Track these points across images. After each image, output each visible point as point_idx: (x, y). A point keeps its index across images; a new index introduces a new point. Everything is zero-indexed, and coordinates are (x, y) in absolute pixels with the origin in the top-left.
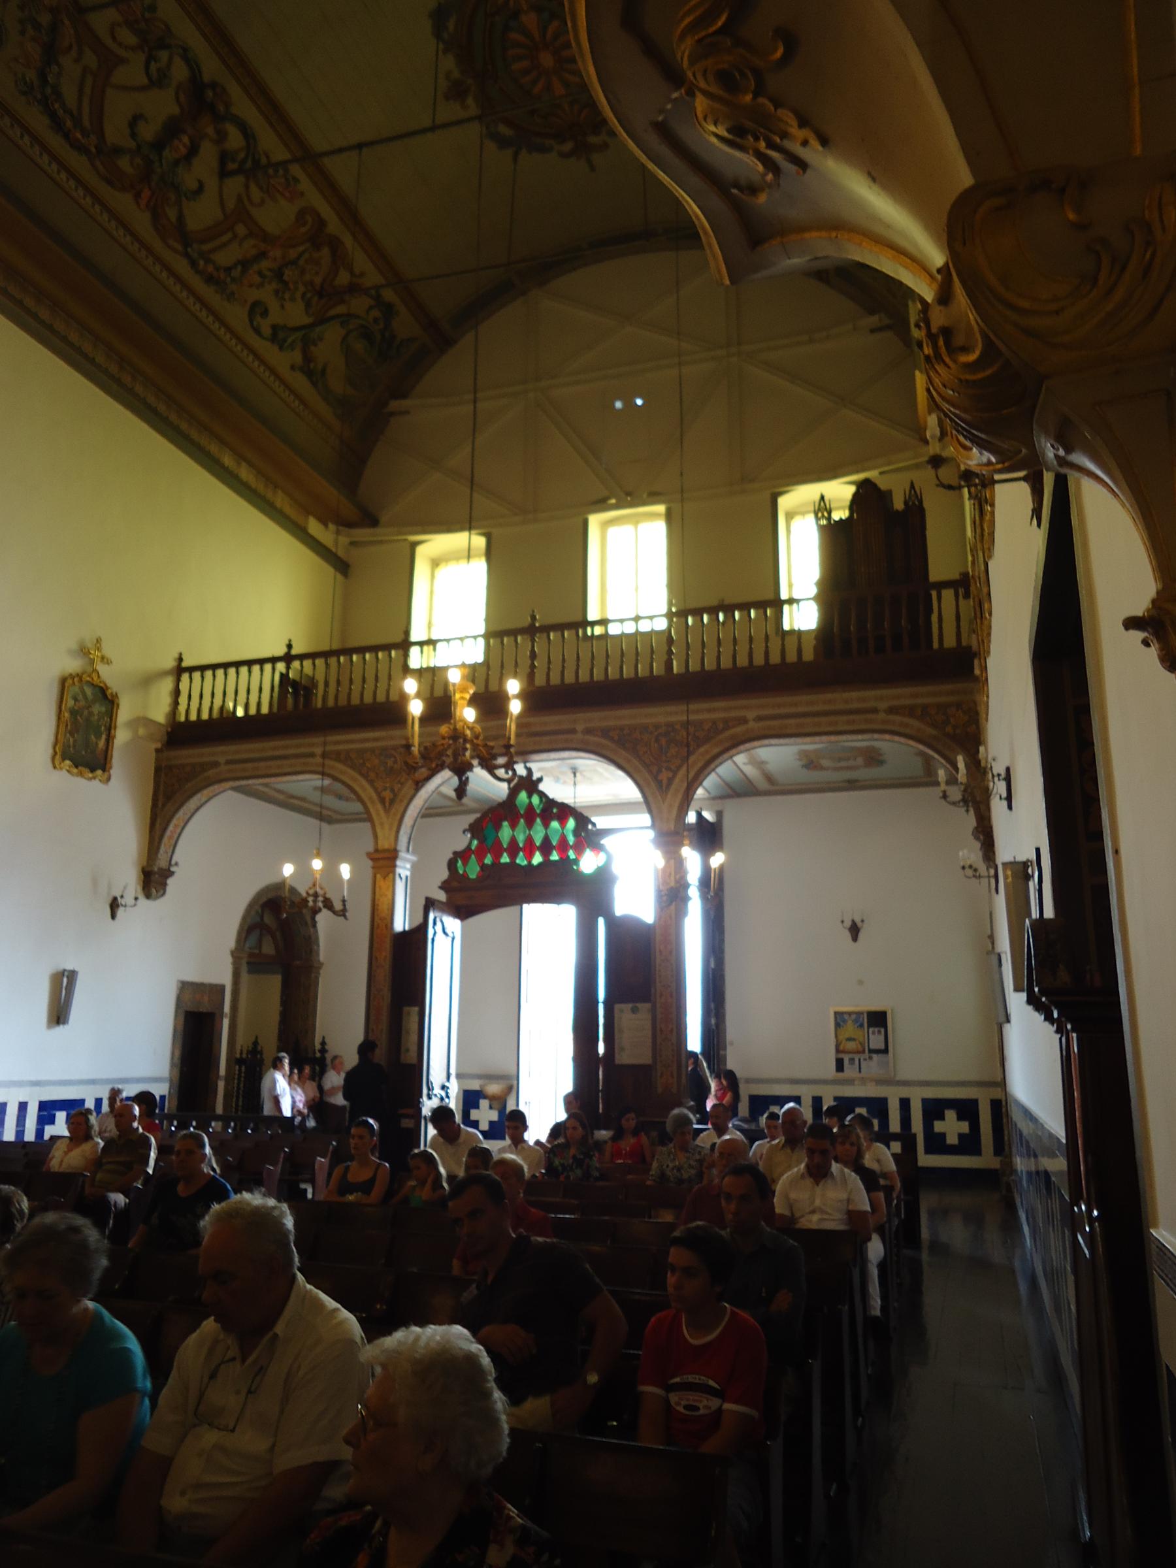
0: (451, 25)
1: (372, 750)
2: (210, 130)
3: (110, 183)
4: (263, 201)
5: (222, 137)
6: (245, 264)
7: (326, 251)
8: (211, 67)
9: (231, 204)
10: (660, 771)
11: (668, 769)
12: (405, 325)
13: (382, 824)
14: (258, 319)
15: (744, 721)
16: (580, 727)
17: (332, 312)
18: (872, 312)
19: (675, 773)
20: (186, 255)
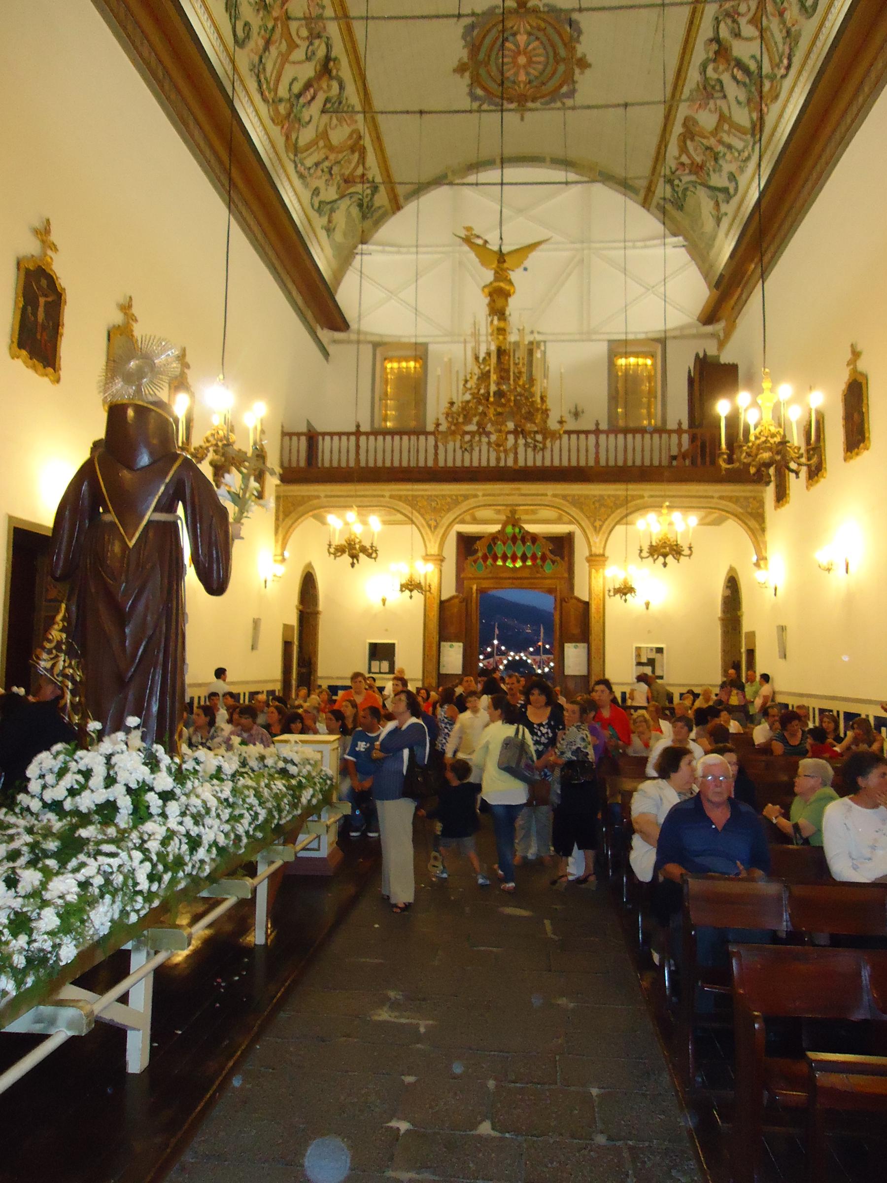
0: (475, 32)
1: (422, 496)
2: (325, 86)
3: (273, 120)
4: (336, 125)
5: (329, 87)
6: (317, 164)
7: (356, 155)
8: (338, 50)
9: (321, 129)
10: (595, 521)
11: (600, 520)
12: (382, 199)
13: (430, 541)
14: (315, 197)
15: (642, 497)
16: (550, 493)
17: (347, 192)
18: (675, 235)
19: (604, 522)
20: (295, 162)
